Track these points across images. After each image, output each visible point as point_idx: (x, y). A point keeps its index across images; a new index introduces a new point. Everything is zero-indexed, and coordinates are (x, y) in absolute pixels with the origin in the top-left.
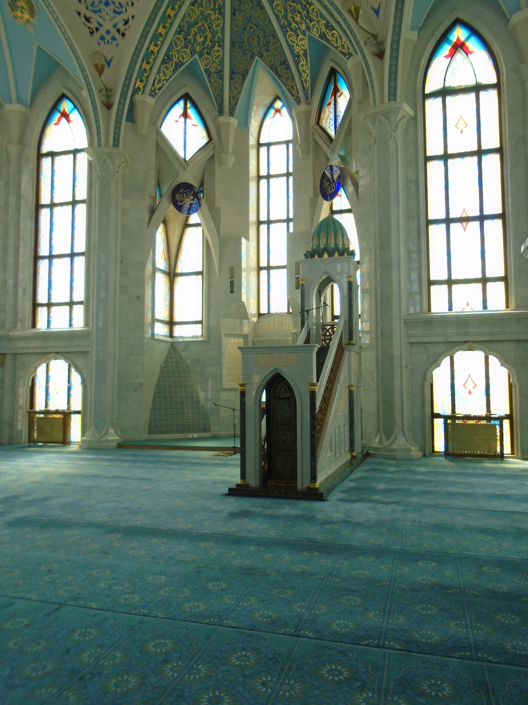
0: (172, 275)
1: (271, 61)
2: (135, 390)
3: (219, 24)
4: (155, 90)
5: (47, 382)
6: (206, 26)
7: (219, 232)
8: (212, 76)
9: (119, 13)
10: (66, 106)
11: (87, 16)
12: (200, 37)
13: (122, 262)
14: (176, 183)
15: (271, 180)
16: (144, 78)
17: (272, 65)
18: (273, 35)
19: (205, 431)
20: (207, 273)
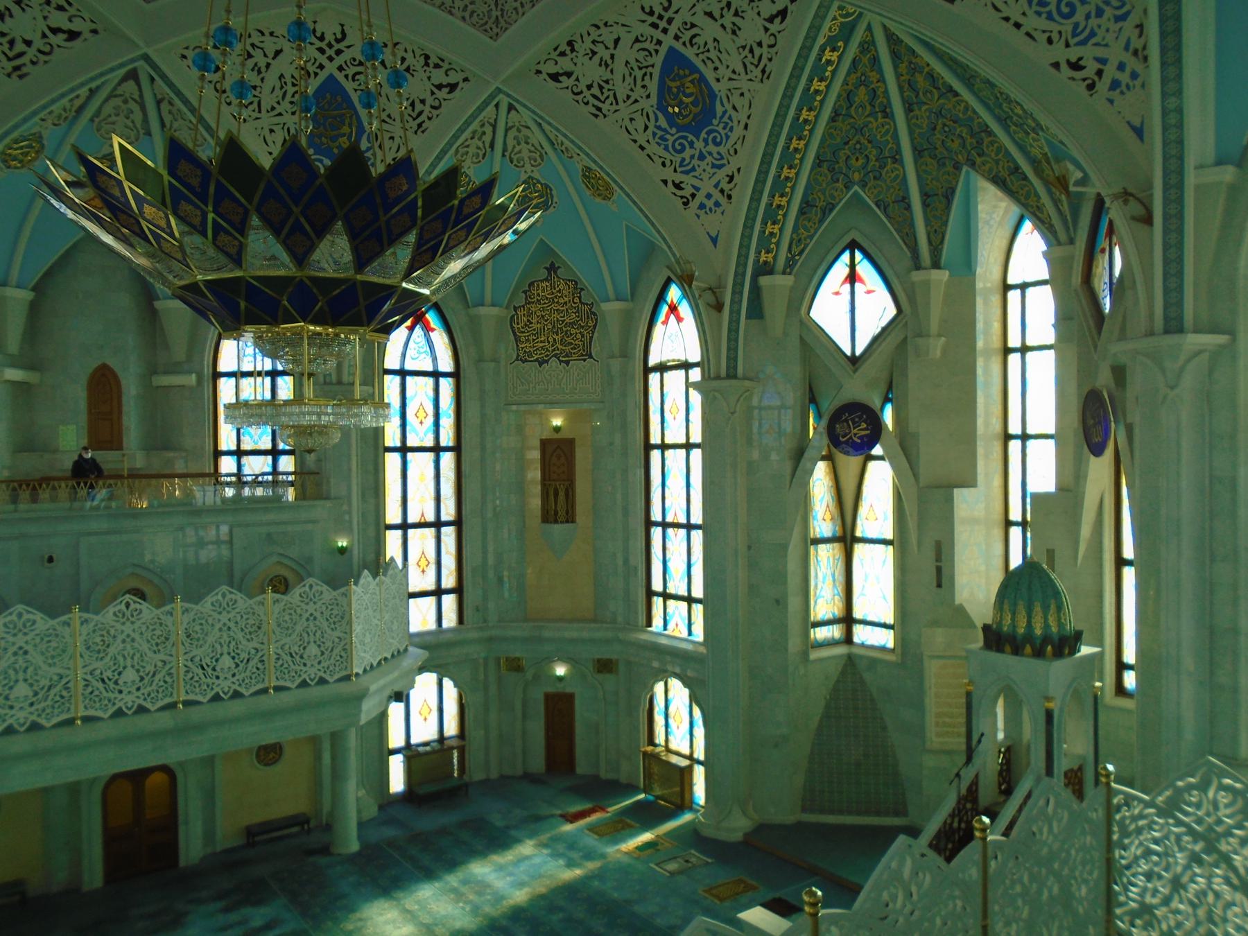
0: (847, 539)
1: (990, 170)
2: (776, 746)
3: (887, 131)
4: (794, 256)
5: (667, 707)
6: (862, 141)
7: (916, 476)
8: (890, 209)
9: (720, 167)
10: (674, 293)
11: (677, 182)
12: (857, 159)
13: (749, 548)
14: (838, 403)
15: (1029, 355)
16: (773, 246)
17: (996, 176)
18: (985, 131)
19: (897, 814)
20: (899, 542)
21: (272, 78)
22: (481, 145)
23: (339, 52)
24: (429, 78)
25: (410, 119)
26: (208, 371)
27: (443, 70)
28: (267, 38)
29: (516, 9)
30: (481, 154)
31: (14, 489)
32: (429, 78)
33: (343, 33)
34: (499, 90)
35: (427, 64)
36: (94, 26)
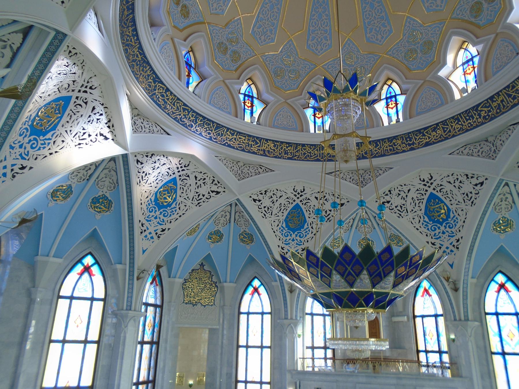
21: (409, 200)
22: (507, 203)
23: (432, 184)
24: (471, 183)
25: (468, 201)
26: (411, 315)
27: (475, 179)
28: (404, 186)
29: (501, 144)
30: (509, 207)
31: (342, 363)
32: (471, 183)
33: (431, 176)
34: (501, 181)
35: (468, 178)
36: (348, 200)
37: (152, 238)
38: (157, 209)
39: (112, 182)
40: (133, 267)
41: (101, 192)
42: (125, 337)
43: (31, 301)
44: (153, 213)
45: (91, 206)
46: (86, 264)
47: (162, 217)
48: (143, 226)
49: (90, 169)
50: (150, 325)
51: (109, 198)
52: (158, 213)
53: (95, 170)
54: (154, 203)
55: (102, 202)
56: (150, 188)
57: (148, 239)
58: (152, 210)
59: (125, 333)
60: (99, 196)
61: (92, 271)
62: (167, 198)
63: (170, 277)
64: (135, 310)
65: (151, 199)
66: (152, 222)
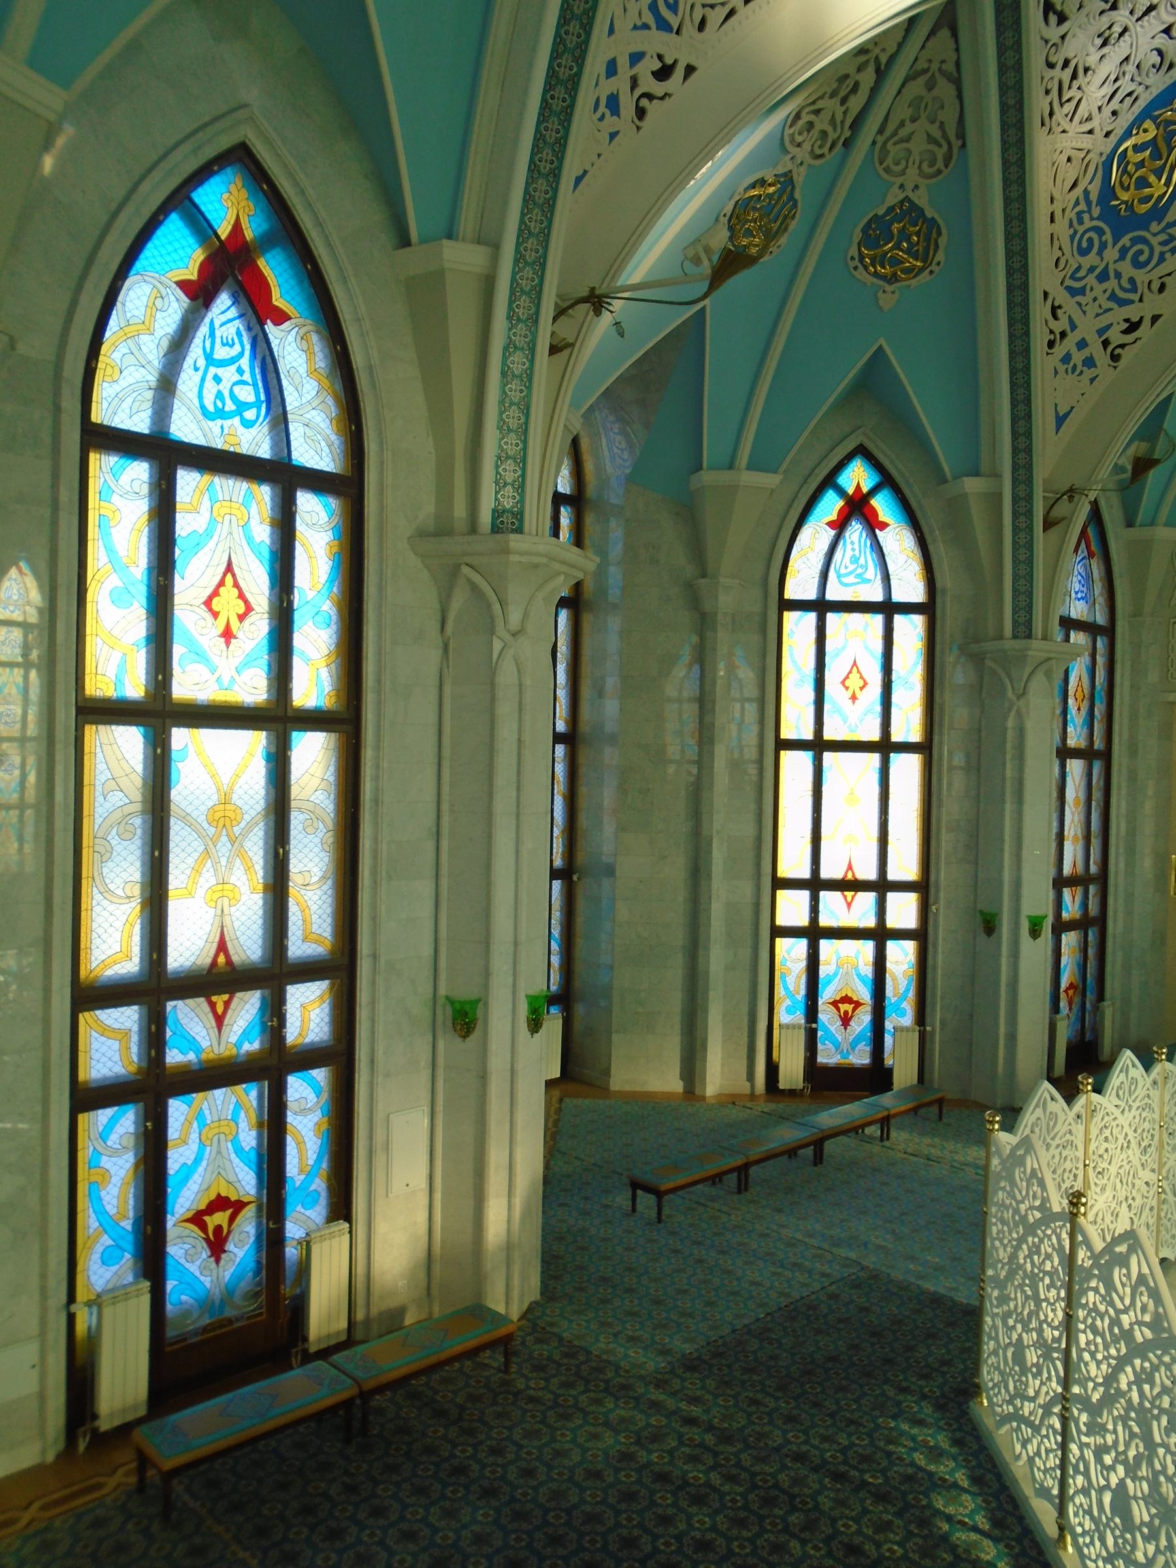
37: (1090, 362)
38: (1108, 237)
39: (937, 134)
40: (1029, 481)
41: (895, 189)
42: (1021, 732)
43: (704, 622)
44: (1092, 259)
45: (862, 258)
46: (851, 491)
47: (1127, 269)
48: (1055, 317)
49: (855, 88)
50: (1079, 695)
51: (929, 215)
52: (1111, 254)
53: (874, 91)
54: (1096, 212)
55: (904, 235)
56: (1086, 142)
57: (1074, 368)
58: (1090, 240)
59: (1019, 715)
60: (891, 209)
61: (874, 513)
62: (1152, 179)
63: (1130, 524)
64: (1045, 638)
65: (1086, 193)
66: (1089, 296)
